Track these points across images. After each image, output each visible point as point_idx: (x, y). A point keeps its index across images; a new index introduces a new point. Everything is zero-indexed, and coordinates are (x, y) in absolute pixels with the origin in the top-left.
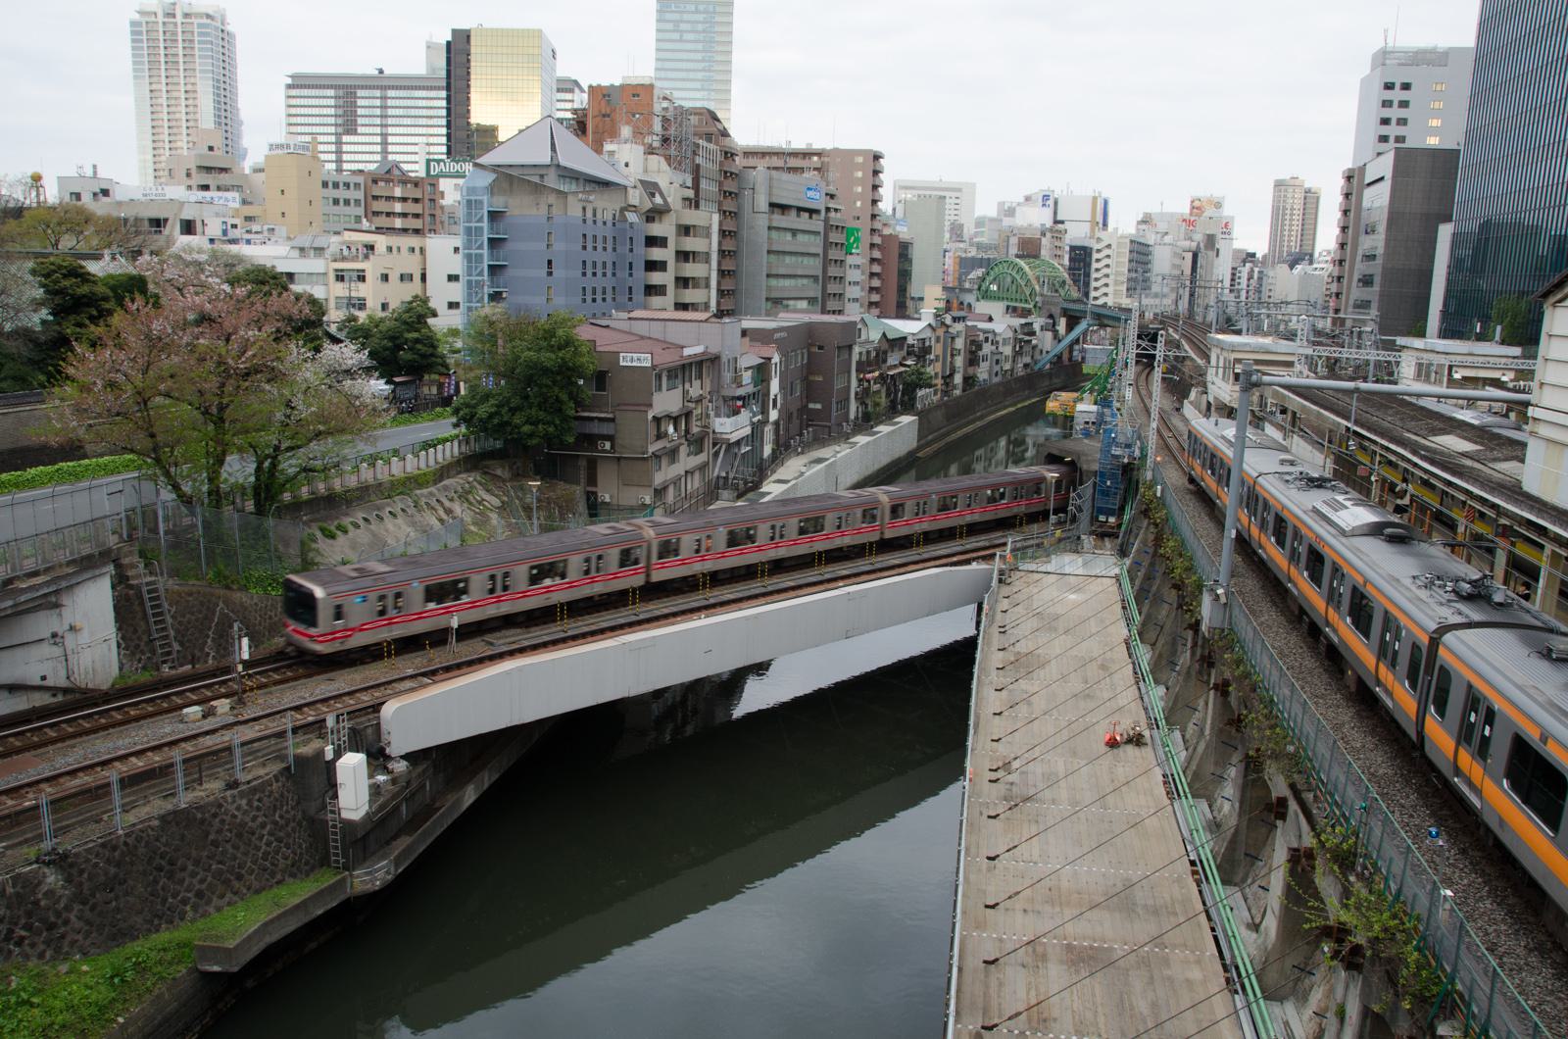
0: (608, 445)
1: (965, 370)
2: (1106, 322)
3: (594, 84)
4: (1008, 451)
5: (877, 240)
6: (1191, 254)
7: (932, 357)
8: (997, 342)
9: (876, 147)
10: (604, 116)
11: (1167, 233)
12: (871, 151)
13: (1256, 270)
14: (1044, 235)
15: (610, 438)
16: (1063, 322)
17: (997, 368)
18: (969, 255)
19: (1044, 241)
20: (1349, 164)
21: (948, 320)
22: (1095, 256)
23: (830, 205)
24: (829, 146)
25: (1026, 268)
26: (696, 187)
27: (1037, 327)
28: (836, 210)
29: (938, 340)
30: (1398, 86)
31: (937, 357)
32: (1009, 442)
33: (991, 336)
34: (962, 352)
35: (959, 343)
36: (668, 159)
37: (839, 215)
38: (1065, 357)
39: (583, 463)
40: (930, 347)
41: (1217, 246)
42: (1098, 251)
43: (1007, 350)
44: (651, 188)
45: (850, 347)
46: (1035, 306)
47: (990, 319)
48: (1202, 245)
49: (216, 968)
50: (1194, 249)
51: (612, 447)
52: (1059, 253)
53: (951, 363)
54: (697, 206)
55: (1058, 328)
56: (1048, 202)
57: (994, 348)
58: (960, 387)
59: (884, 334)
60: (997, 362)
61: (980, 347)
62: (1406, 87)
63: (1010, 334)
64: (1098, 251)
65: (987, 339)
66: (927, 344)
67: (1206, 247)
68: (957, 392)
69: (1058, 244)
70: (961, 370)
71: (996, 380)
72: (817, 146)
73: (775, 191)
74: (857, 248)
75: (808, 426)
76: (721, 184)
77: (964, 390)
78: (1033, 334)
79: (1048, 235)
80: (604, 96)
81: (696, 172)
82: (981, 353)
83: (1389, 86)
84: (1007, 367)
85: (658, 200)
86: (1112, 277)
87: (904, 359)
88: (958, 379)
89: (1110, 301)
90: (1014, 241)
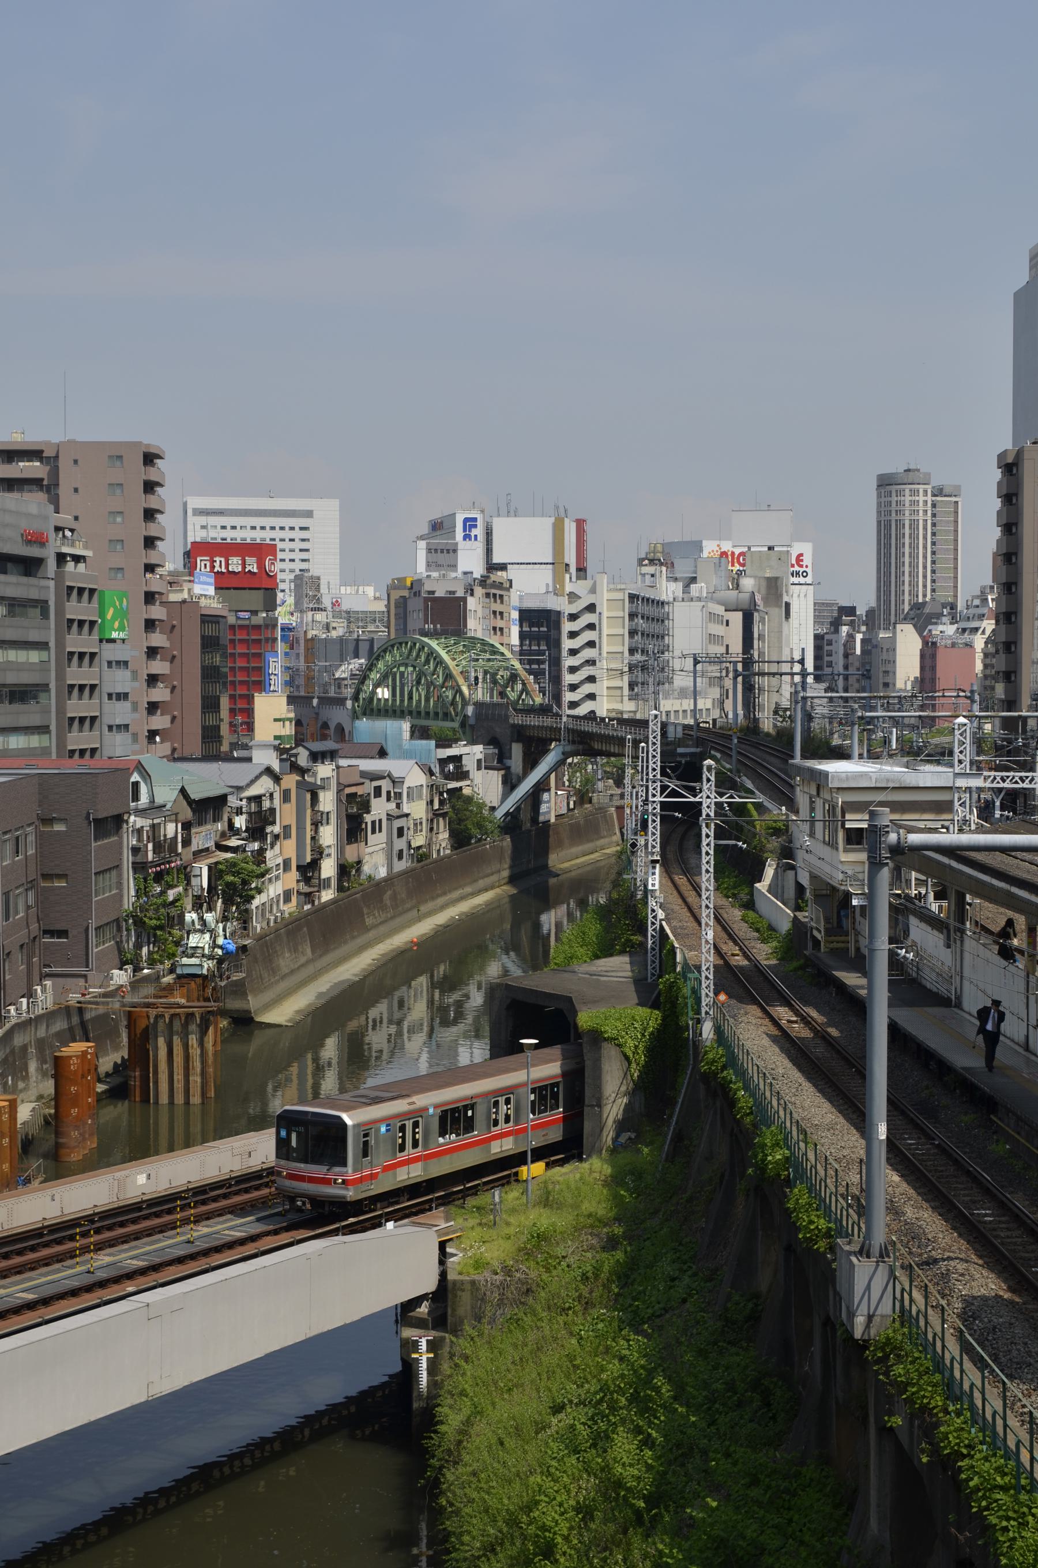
1: (341, 851)
2: (597, 746)
4: (431, 1002)
5: (157, 612)
6: (740, 614)
7: (277, 829)
8: (398, 796)
9: (152, 440)
11: (693, 580)
12: (137, 444)
13: (859, 637)
14: (472, 595)
16: (517, 750)
17: (400, 844)
18: (334, 634)
19: (472, 603)
20: (1006, 443)
21: (303, 758)
22: (567, 626)
23: (65, 550)
25: (443, 654)
27: (469, 764)
28: (77, 559)
29: (286, 796)
31: (286, 829)
32: (433, 986)
33: (385, 785)
35: (327, 801)
37: (81, 566)
38: (525, 816)
40: (272, 810)
41: (786, 599)
42: (573, 617)
43: (418, 809)
45: (118, 821)
46: (463, 725)
47: (382, 753)
48: (758, 598)
50: (746, 607)
52: (500, 623)
53: (313, 838)
55: (508, 762)
56: (474, 532)
57: (392, 806)
58: (334, 883)
59: (183, 791)
60: (401, 832)
61: (366, 807)
64: (573, 617)
65: (378, 792)
66: (266, 804)
67: (766, 600)
68: (327, 895)
69: (498, 607)
70: (333, 851)
71: (400, 866)
74: (121, 629)
75: (43, 976)
77: (340, 889)
78: (463, 775)
82: (368, 818)
84: (419, 840)
86: (604, 664)
88: (328, 869)
89: (603, 707)
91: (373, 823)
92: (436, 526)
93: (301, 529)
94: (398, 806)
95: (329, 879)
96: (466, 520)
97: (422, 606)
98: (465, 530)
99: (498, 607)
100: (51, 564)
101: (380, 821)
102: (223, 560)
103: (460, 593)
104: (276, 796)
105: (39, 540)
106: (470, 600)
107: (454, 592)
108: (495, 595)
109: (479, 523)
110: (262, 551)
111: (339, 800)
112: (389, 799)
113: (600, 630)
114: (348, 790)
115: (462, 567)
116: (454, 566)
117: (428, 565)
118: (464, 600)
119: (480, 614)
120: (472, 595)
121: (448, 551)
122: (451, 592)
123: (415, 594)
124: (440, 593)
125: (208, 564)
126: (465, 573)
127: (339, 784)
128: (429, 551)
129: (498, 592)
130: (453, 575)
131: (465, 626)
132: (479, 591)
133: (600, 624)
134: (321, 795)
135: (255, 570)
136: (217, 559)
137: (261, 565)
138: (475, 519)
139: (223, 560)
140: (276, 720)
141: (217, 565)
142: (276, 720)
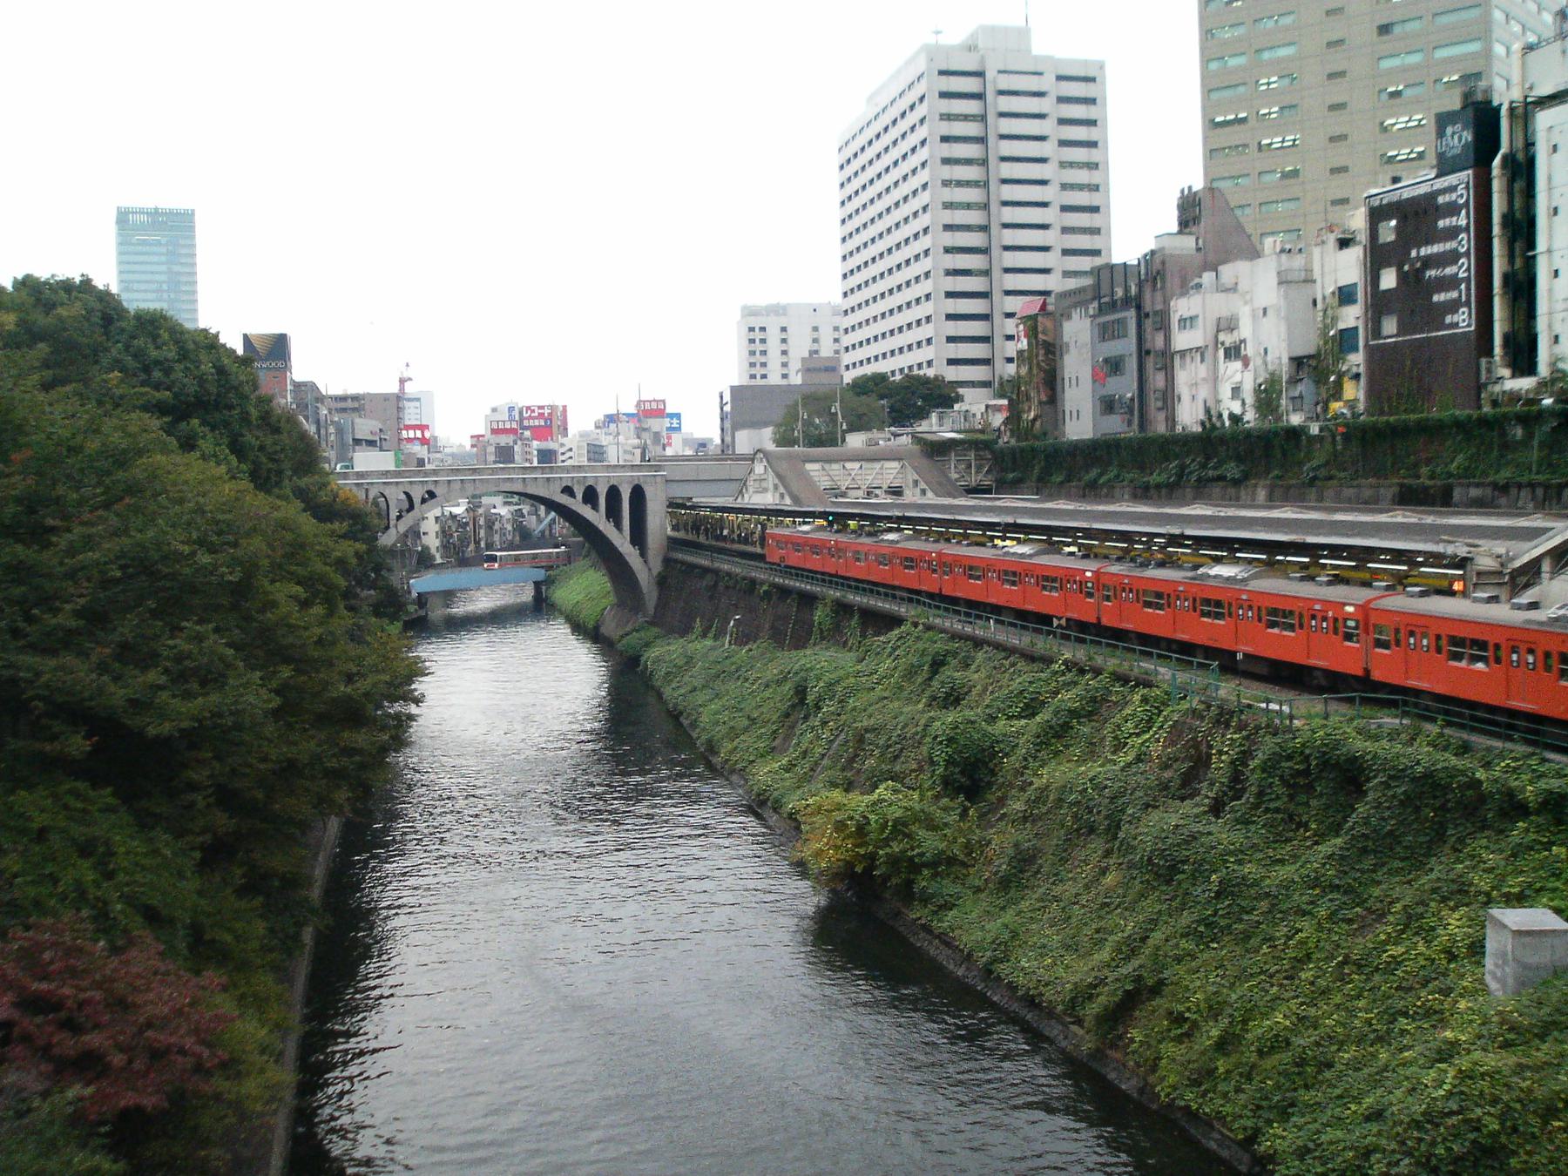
19: (516, 448)
24: (361, 392)
27: (525, 512)
30: (757, 330)
35: (482, 521)
38: (547, 533)
43: (509, 527)
62: (763, 329)
63: (510, 516)
69: (527, 449)
72: (352, 391)
78: (523, 516)
79: (519, 442)
83: (752, 329)
84: (510, 538)
90: (491, 449)
92: (494, 410)
99: (527, 449)
110: (423, 428)
124: (503, 444)
132: (519, 442)
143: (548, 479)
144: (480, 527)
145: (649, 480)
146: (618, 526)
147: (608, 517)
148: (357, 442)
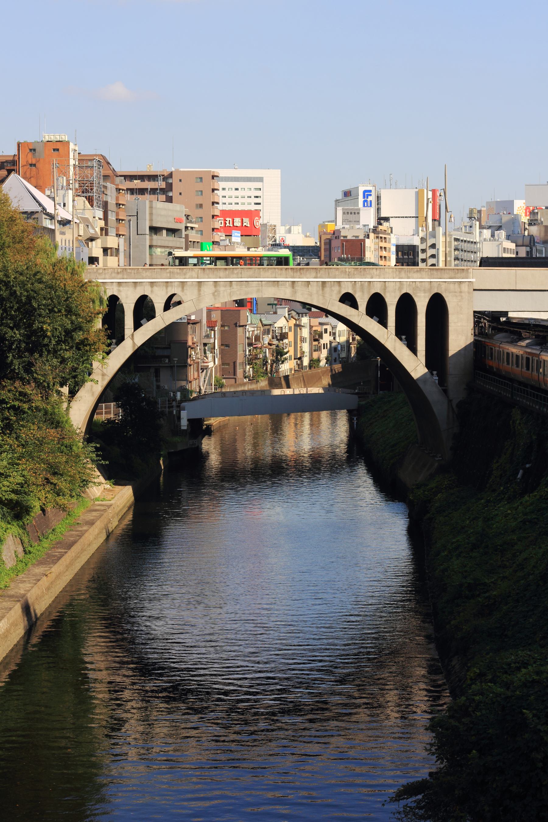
0: (167, 361)
1: (311, 354)
3: (22, 141)
8: (334, 334)
10: (31, 165)
14: (368, 238)
15: (168, 357)
22: (421, 256)
23: (189, 225)
26: (105, 218)
28: (192, 228)
29: (290, 329)
33: (329, 329)
34: (308, 340)
35: (305, 333)
36: (90, 200)
39: (152, 370)
44: (88, 224)
49: (172, 451)
51: (169, 361)
52: (384, 253)
54: (107, 234)
56: (370, 198)
57: (332, 338)
61: (321, 336)
64: (424, 251)
69: (383, 244)
73: (154, 217)
76: (117, 214)
79: (372, 235)
80: (31, 150)
81: (105, 206)
85: (92, 231)
87: (270, 340)
88: (306, 362)
91: (324, 344)
92: (347, 194)
93: (256, 189)
94: (334, 338)
95: (306, 366)
96: (365, 192)
97: (340, 245)
98: (364, 197)
99: (383, 244)
100: (184, 230)
101: (327, 344)
102: (231, 219)
103: (361, 237)
104: (287, 327)
105: (179, 221)
106: (367, 240)
107: (358, 237)
108: (381, 238)
109: (373, 193)
110: (252, 215)
111: (311, 333)
112: (330, 335)
113: (438, 258)
114: (314, 329)
115: (363, 221)
116: (358, 222)
117: (344, 221)
118: (364, 241)
119: (373, 249)
120: (368, 238)
121: (355, 213)
122: (356, 237)
123: (336, 238)
125: (223, 222)
126: (364, 226)
127: (310, 326)
128: (344, 213)
129: (383, 236)
130: (358, 227)
131: (365, 256)
132: (372, 235)
133: (438, 255)
134: (303, 329)
135: (248, 225)
136: (228, 219)
137: (252, 222)
138: (370, 191)
139: (231, 219)
140: (268, 304)
141: (227, 222)
142: (268, 304)
143: (324, 283)
144: (303, 340)
145: (452, 286)
146: (412, 347)
147: (399, 334)
148: (154, 230)
